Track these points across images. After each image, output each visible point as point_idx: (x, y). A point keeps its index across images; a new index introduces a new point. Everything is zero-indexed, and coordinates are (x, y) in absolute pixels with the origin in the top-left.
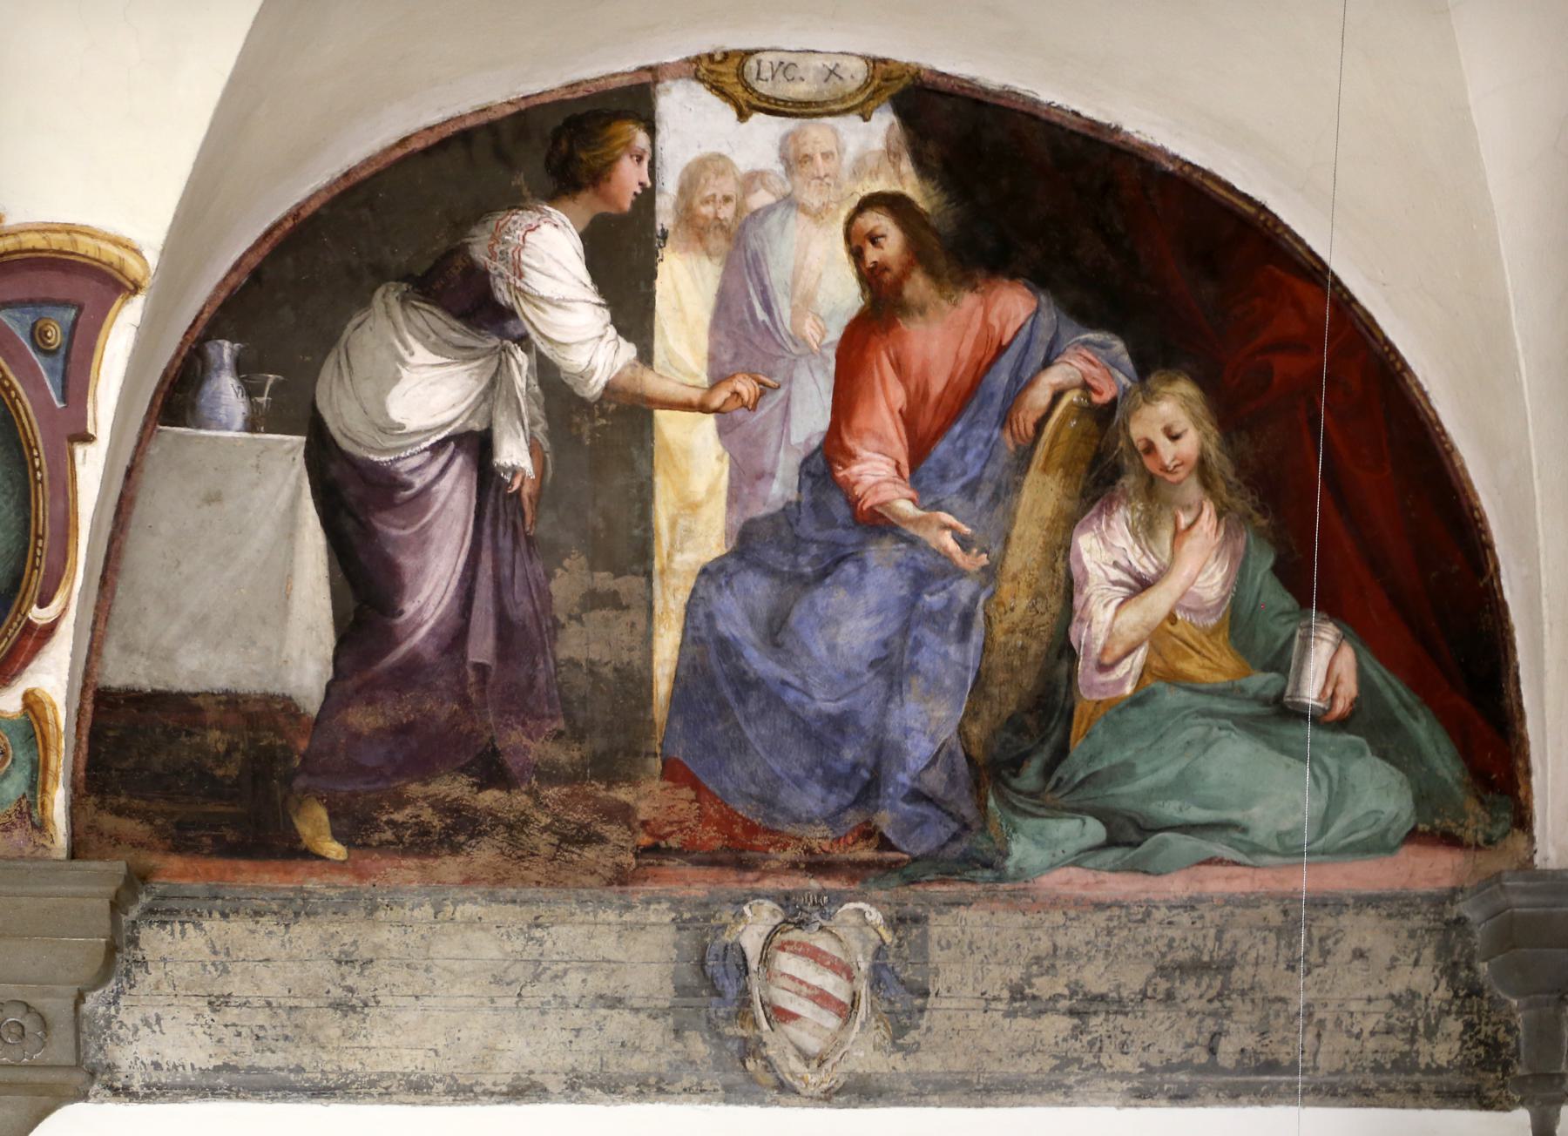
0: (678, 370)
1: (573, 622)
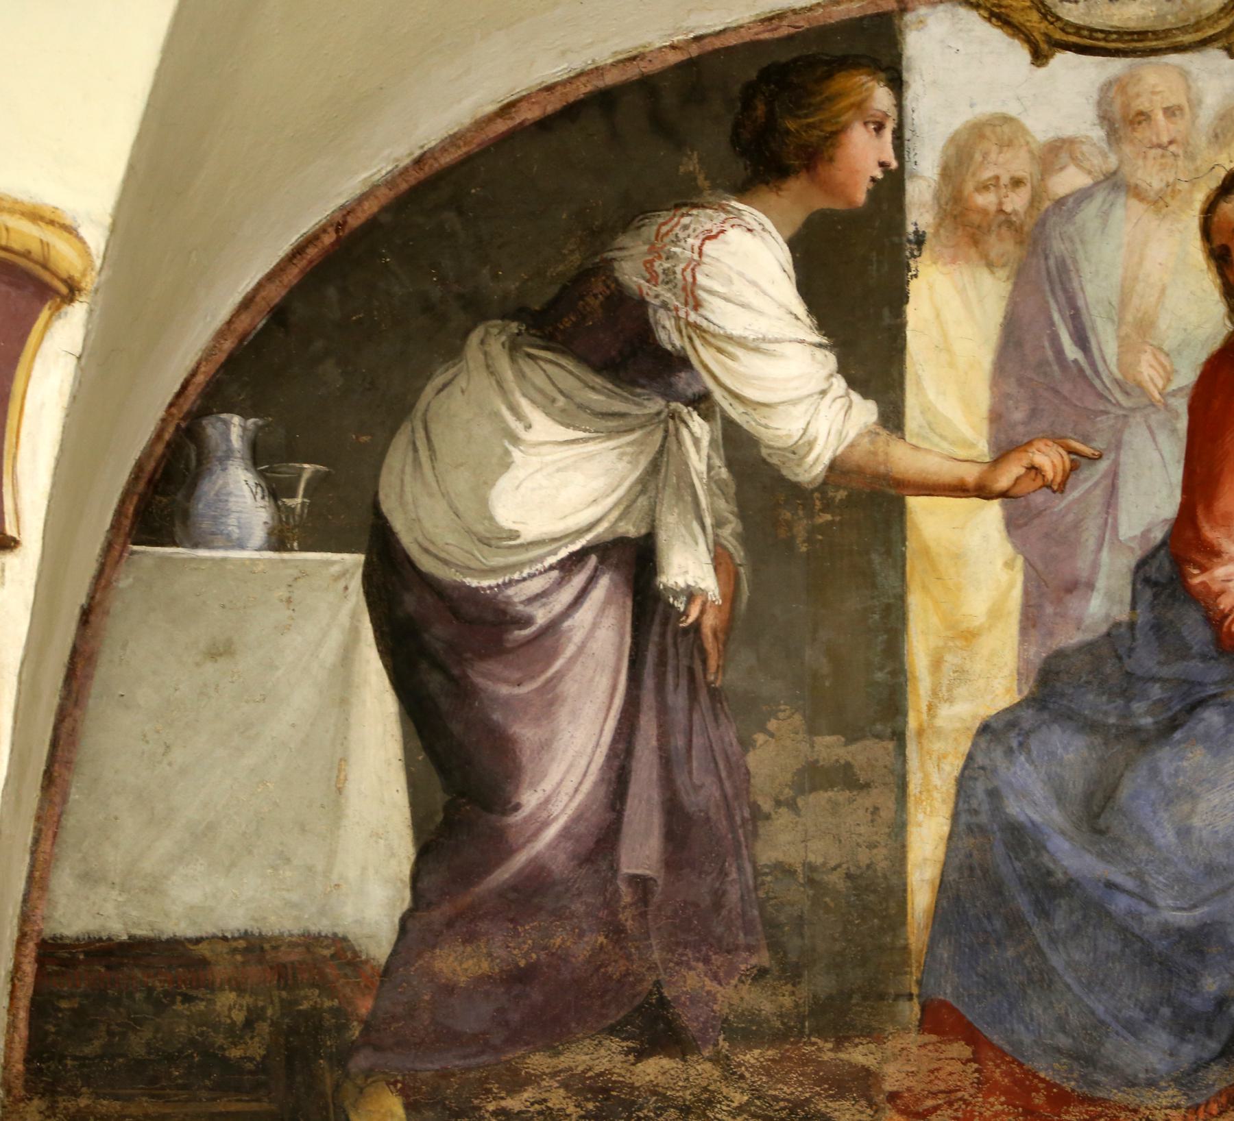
0: (942, 437)
1: (783, 810)
